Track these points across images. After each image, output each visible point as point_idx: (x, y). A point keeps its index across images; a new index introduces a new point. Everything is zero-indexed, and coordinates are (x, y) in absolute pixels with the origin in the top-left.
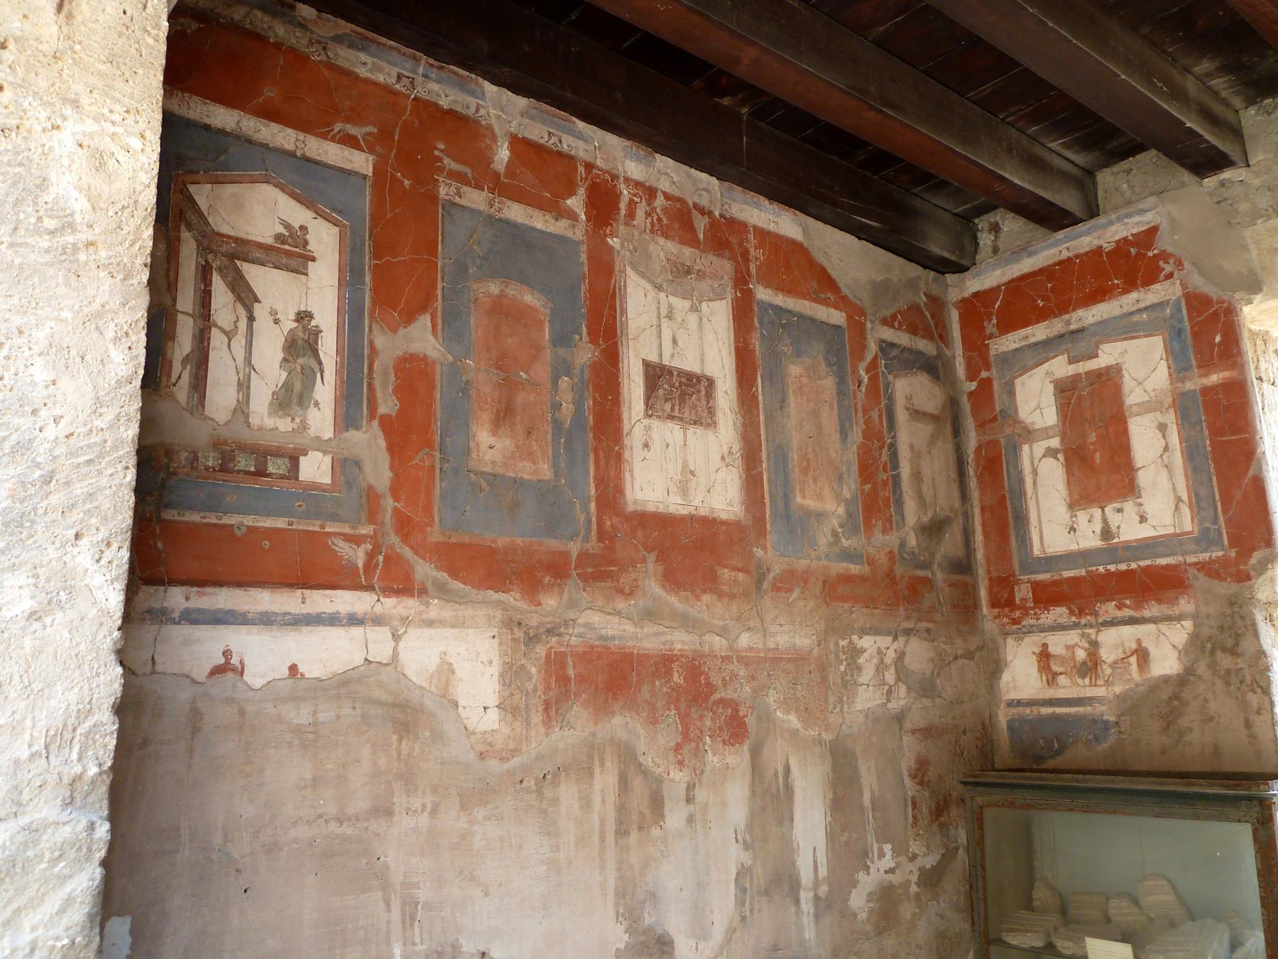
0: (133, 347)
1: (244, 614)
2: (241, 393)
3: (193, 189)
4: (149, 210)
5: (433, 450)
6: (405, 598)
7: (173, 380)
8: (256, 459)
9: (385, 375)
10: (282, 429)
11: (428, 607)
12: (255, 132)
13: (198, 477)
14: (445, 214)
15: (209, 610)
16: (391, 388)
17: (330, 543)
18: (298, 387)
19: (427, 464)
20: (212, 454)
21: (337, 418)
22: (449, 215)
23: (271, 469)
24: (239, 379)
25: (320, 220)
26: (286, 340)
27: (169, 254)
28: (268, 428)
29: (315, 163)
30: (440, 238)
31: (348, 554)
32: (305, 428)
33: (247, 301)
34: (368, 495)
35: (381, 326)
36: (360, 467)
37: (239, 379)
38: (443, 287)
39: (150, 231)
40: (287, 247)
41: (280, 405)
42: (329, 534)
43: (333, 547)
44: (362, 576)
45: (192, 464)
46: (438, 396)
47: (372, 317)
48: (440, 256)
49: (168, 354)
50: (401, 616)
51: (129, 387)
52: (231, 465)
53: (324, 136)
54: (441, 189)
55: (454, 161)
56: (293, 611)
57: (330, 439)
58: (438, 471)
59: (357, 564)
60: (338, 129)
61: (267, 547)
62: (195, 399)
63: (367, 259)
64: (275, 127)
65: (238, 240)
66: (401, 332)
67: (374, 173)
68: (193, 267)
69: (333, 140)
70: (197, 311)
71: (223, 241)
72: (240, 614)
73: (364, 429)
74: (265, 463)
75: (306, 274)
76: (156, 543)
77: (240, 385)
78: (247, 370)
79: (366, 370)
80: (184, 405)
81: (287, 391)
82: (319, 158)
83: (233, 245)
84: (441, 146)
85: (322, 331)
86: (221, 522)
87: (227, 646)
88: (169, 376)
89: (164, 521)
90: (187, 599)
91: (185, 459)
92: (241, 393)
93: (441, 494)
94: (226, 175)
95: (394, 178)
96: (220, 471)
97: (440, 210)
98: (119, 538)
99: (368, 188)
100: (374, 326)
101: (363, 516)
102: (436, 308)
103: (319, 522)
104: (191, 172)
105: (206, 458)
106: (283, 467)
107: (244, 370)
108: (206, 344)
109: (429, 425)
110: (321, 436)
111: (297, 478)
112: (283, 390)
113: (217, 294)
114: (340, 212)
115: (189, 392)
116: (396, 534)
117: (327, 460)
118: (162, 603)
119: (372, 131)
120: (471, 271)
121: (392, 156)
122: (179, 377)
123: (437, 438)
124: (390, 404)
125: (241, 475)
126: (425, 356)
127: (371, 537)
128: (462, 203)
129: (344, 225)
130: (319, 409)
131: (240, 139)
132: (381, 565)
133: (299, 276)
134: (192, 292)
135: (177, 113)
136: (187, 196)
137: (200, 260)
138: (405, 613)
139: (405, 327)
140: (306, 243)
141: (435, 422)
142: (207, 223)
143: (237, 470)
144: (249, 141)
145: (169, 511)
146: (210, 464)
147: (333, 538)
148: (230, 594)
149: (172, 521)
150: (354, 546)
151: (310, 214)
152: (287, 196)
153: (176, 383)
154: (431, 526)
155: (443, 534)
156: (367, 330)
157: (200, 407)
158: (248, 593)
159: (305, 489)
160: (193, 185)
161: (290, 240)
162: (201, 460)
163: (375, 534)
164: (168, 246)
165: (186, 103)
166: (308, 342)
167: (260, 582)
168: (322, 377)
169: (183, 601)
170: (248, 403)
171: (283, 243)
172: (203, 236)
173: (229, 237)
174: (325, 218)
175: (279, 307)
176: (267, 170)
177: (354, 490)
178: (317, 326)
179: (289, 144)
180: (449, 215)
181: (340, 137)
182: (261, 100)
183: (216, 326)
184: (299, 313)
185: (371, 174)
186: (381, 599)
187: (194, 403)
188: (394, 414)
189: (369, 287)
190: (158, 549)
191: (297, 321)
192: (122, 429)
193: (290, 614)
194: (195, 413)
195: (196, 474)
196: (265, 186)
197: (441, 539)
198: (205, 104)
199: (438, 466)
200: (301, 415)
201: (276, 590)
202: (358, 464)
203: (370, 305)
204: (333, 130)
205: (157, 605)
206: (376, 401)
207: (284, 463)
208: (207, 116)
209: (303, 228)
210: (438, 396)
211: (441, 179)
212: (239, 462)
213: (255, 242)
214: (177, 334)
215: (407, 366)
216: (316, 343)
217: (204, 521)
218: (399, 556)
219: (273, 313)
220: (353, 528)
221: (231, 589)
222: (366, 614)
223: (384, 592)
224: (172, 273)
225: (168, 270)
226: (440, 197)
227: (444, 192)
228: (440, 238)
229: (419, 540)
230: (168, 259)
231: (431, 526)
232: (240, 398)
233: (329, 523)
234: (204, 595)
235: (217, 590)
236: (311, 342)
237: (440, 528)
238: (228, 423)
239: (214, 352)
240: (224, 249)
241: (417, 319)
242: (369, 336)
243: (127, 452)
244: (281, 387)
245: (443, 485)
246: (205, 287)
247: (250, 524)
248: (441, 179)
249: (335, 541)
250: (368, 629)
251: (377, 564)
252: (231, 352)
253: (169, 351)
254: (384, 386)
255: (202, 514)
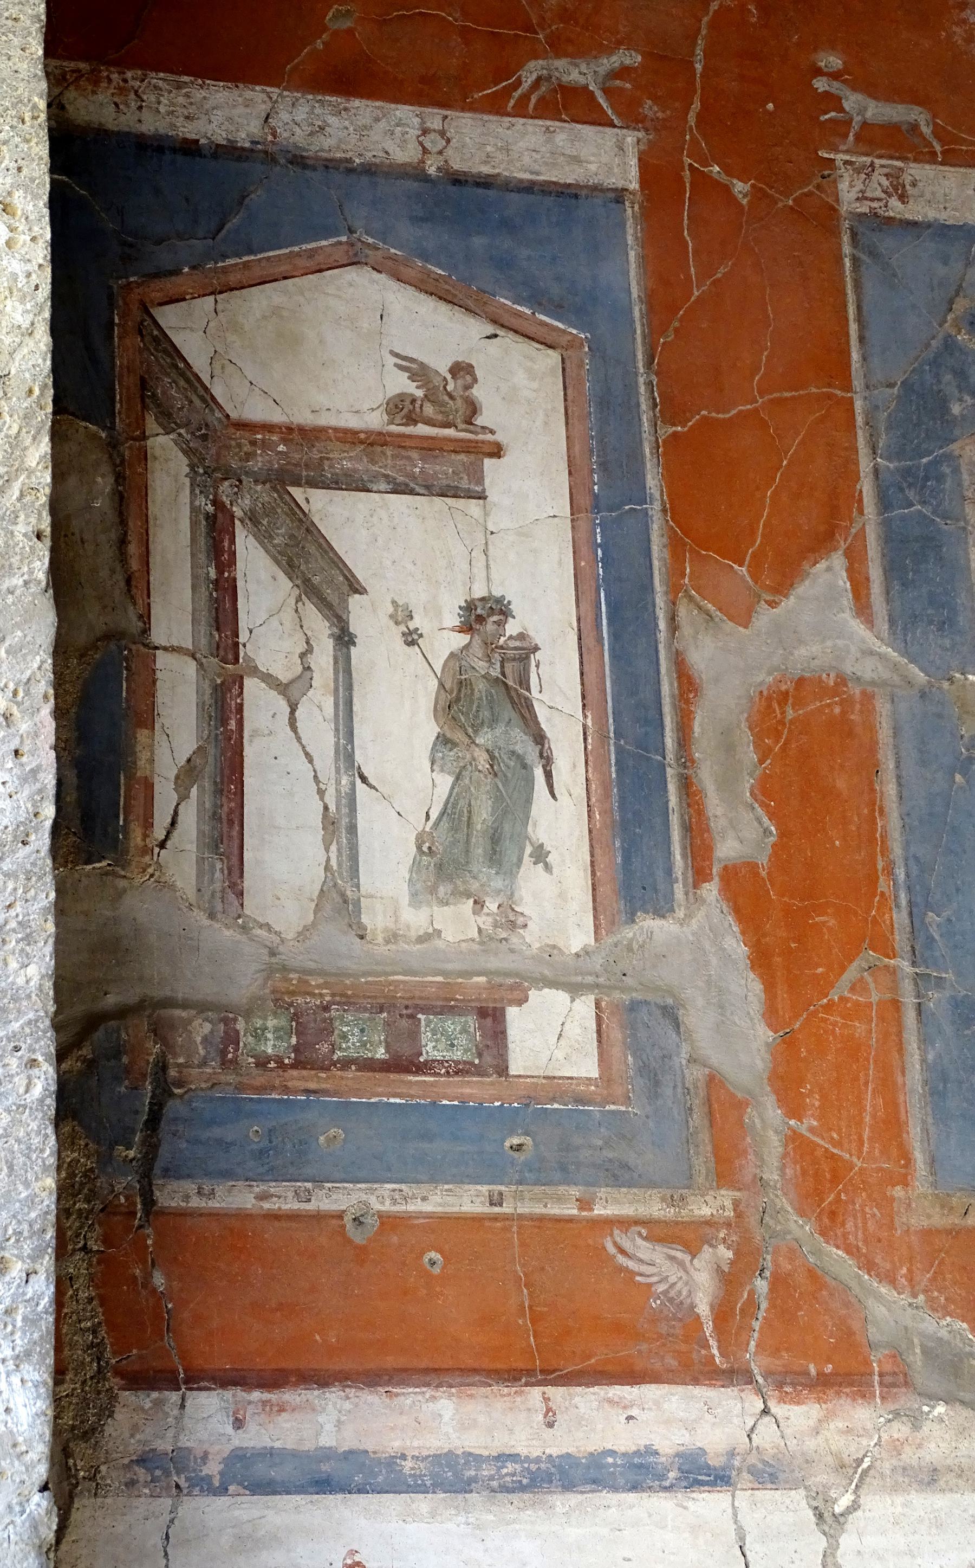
0: (25, 749)
1: (392, 1462)
2: (334, 848)
3: (168, 317)
4: (37, 392)
5: (887, 949)
6: (844, 1403)
7: (159, 833)
8: (387, 1024)
9: (730, 749)
10: (450, 935)
11: (916, 1427)
12: (311, 134)
13: (240, 1088)
14: (864, 257)
15: (295, 1454)
16: (748, 783)
17: (611, 1249)
18: (484, 814)
19: (875, 998)
20: (271, 1023)
21: (601, 889)
22: (873, 254)
23: (431, 1050)
24: (326, 808)
25: (508, 340)
26: (441, 685)
27: (122, 497)
28: (413, 934)
29: (478, 184)
30: (853, 328)
31: (664, 1279)
32: (512, 925)
33: (328, 592)
34: (708, 1101)
35: (700, 608)
36: (677, 1025)
37: (326, 808)
38: (876, 471)
39: (45, 445)
40: (422, 429)
41: (440, 867)
42: (609, 1223)
43: (621, 1259)
44: (713, 1343)
45: (224, 1053)
46: (891, 789)
47: (674, 590)
48: (858, 383)
49: (142, 763)
50: (837, 1456)
51: (23, 852)
52: (324, 1048)
53: (495, 106)
54: (843, 186)
55: (876, 98)
56: (522, 1450)
57: (587, 952)
58: (910, 1017)
59: (692, 1307)
60: (534, 76)
61: (436, 1270)
62: (218, 874)
63: (646, 425)
64: (363, 109)
65: (290, 432)
66: (764, 617)
67: (643, 181)
68: (185, 524)
69: (521, 111)
70: (204, 641)
71: (253, 443)
72: (379, 1462)
73: (680, 913)
74: (414, 1035)
75: (482, 497)
76: (148, 1276)
77: (329, 823)
78: (345, 781)
79: (670, 741)
80: (191, 895)
81: (454, 829)
82: (486, 170)
83: (281, 448)
84: (832, 61)
85: (536, 649)
86: (311, 1207)
87: (353, 1552)
88: (148, 824)
89: (163, 1213)
90: (239, 1424)
91: (205, 1040)
92: (334, 848)
93: (926, 1082)
94: (246, 265)
95: (700, 179)
96: (296, 1065)
97: (847, 249)
98: (27, 1247)
99: (630, 223)
100: (683, 611)
101: (702, 1162)
102: (862, 534)
103: (575, 1191)
104: (159, 275)
105: (259, 1035)
106: (463, 1040)
107: (338, 782)
108: (233, 725)
109: (873, 881)
110: (561, 945)
111: (502, 1070)
112: (445, 824)
113: (252, 587)
114: (557, 310)
115: (200, 861)
116: (801, 1213)
117: (585, 1007)
118: (176, 1437)
119: (628, 62)
120: (956, 409)
121: (692, 119)
122: (173, 823)
123: (900, 918)
124: (751, 832)
125: (351, 1073)
126: (842, 680)
127: (728, 1225)
128: (909, 216)
129: (574, 344)
130: (548, 868)
131: (274, 161)
132: (764, 1305)
133: (460, 503)
134: (189, 592)
135: (111, 126)
136: (155, 339)
137: (201, 501)
138: (852, 1449)
139: (772, 604)
140: (473, 409)
141: (889, 870)
142: (210, 401)
143: (338, 1061)
144: (298, 160)
145: (174, 1185)
146: (270, 1051)
147: (616, 1232)
148: (347, 1405)
149: (183, 1214)
150: (679, 1255)
151: (477, 328)
152: (411, 291)
153: (168, 834)
154: (906, 1185)
155: (945, 1205)
156: (662, 625)
157: (231, 897)
158: (396, 1401)
159: (529, 1100)
160: (167, 308)
161: (429, 410)
162: (246, 1040)
163: (739, 1215)
164: (119, 478)
165: (132, 96)
166: (498, 682)
167: (426, 1371)
168: (548, 775)
169: (229, 1429)
170: (354, 871)
171: (411, 420)
172: (204, 438)
173: (268, 428)
174: (516, 332)
175: (416, 597)
176: (351, 231)
177: (669, 1092)
178: (522, 636)
179: (403, 144)
180: (873, 254)
181: (541, 100)
182: (319, 45)
183: (254, 671)
184: (470, 607)
185: (634, 185)
186: (772, 1405)
187: (218, 886)
188: (763, 860)
189: (657, 506)
190: (154, 1290)
191: (466, 628)
192: (13, 965)
193: (514, 1457)
194: (219, 916)
195: (231, 1078)
196: (350, 274)
197: (939, 1220)
198: (179, 86)
199: (909, 1000)
200: (498, 892)
201: (473, 1390)
202: (671, 1014)
203: (666, 554)
204: (519, 83)
205: (164, 1445)
206: (708, 830)
207: (464, 1030)
208: (187, 118)
209: (461, 370)
210: (891, 789)
211: (840, 157)
212: (344, 1037)
213: (336, 430)
214: (160, 708)
215: (790, 714)
216: (524, 682)
217: (266, 1205)
218: (812, 1274)
219: (400, 615)
220: (671, 1202)
221: (352, 1392)
222: (732, 1454)
223: (780, 1386)
224: (133, 549)
225: (123, 542)
226: (844, 209)
227: (853, 195)
228: (853, 328)
229: (871, 1226)
230: (121, 514)
231: (905, 1182)
232: (334, 863)
233: (602, 1192)
234: (282, 1410)
235: (313, 1395)
236: (510, 683)
237: (934, 1185)
238: (304, 933)
239: (256, 741)
240: (257, 464)
241: (804, 575)
242: (669, 645)
243: (29, 1022)
244: (439, 819)
245: (930, 1057)
246: (220, 571)
247: (387, 1207)
248: (840, 157)
249: (626, 1244)
250: (743, 1498)
251: (752, 1305)
252: (299, 739)
253: (143, 757)
254: (726, 783)
255: (259, 1188)
